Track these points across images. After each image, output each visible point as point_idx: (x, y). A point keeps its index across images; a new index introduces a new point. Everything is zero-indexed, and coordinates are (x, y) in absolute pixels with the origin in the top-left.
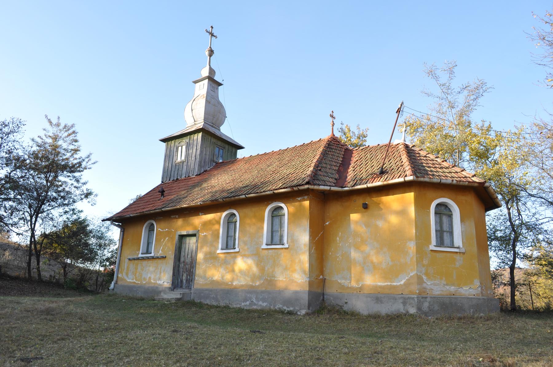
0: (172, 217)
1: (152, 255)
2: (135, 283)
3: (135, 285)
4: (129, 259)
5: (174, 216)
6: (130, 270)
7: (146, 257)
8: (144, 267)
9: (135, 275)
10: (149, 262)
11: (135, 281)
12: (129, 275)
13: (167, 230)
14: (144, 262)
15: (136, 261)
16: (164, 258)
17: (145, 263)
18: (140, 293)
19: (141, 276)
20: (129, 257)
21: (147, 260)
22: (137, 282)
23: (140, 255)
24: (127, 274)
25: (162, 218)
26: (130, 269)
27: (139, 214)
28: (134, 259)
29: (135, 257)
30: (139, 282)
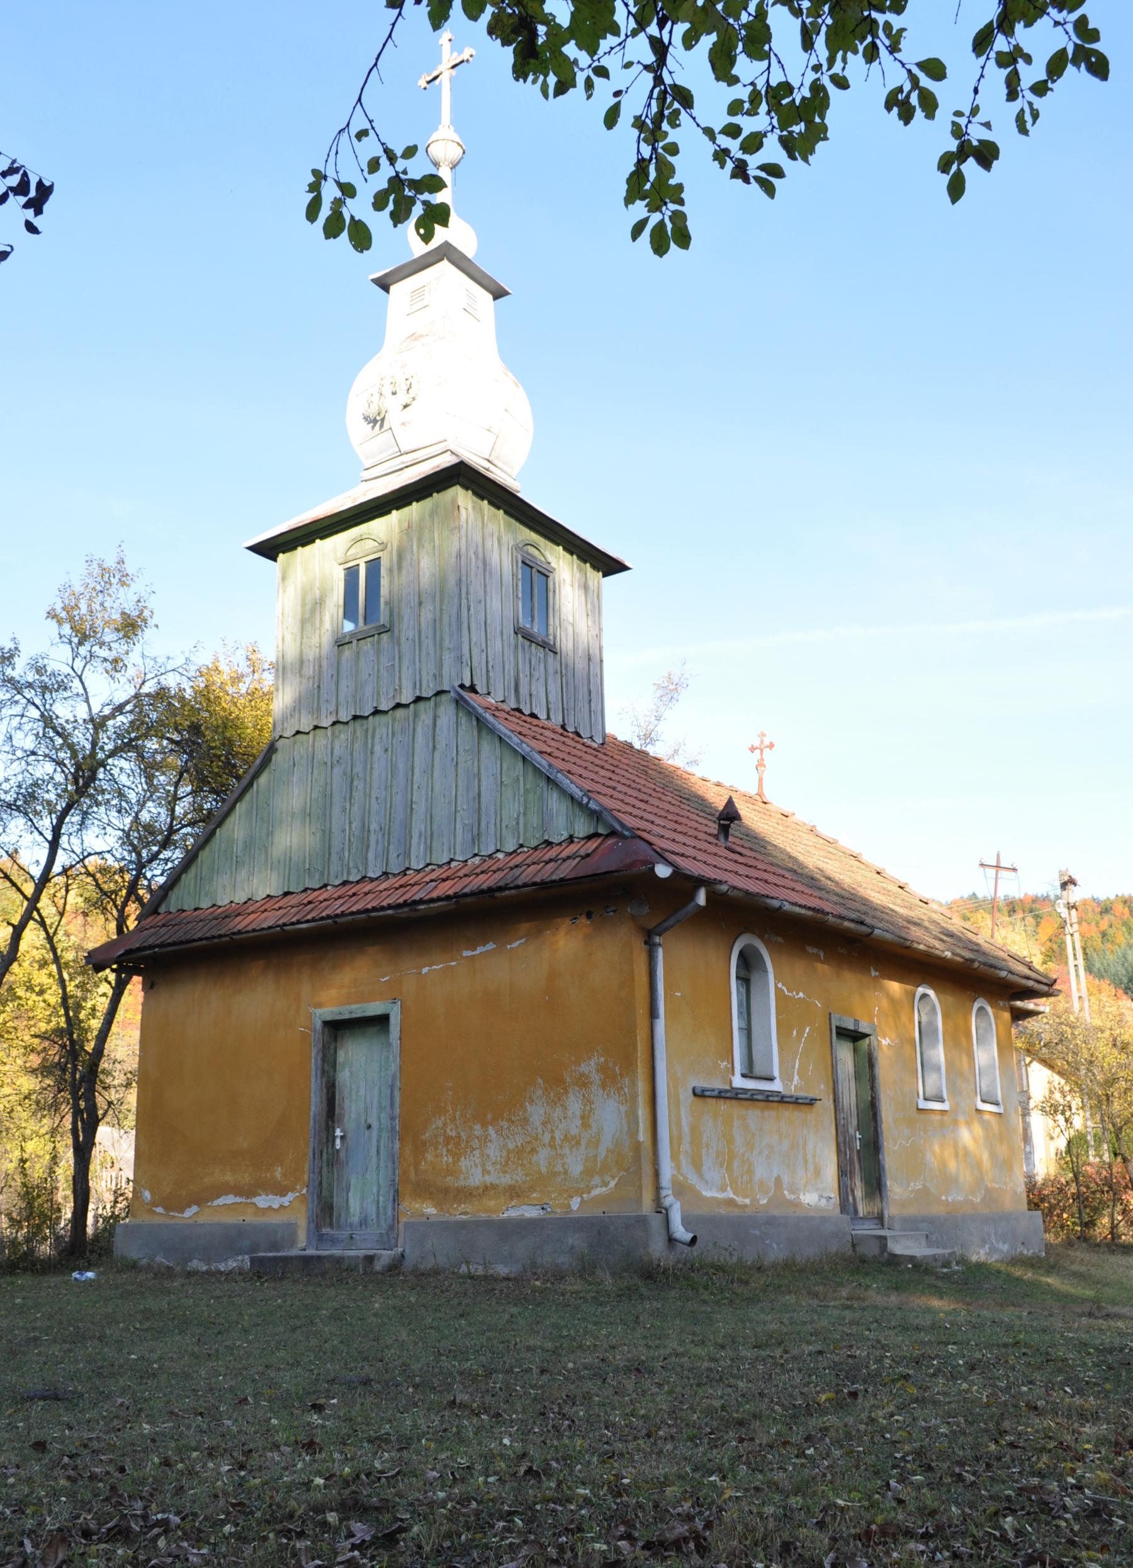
0: (810, 950)
1: (777, 1086)
2: (731, 1202)
3: (736, 1212)
4: (699, 1094)
5: (815, 951)
6: (707, 1146)
7: (761, 1092)
8: (753, 1134)
9: (729, 1169)
10: (766, 1113)
11: (732, 1196)
12: (705, 1168)
13: (801, 995)
14: (750, 1112)
15: (723, 1106)
16: (811, 1102)
17: (753, 1115)
18: (775, 1246)
19: (750, 1172)
20: (702, 1083)
21: (763, 1104)
22: (739, 1200)
23: (738, 1082)
24: (697, 1165)
25: (780, 939)
26: (705, 1140)
27: (810, 913)
28: (721, 1095)
29: (719, 1085)
30: (747, 1201)
